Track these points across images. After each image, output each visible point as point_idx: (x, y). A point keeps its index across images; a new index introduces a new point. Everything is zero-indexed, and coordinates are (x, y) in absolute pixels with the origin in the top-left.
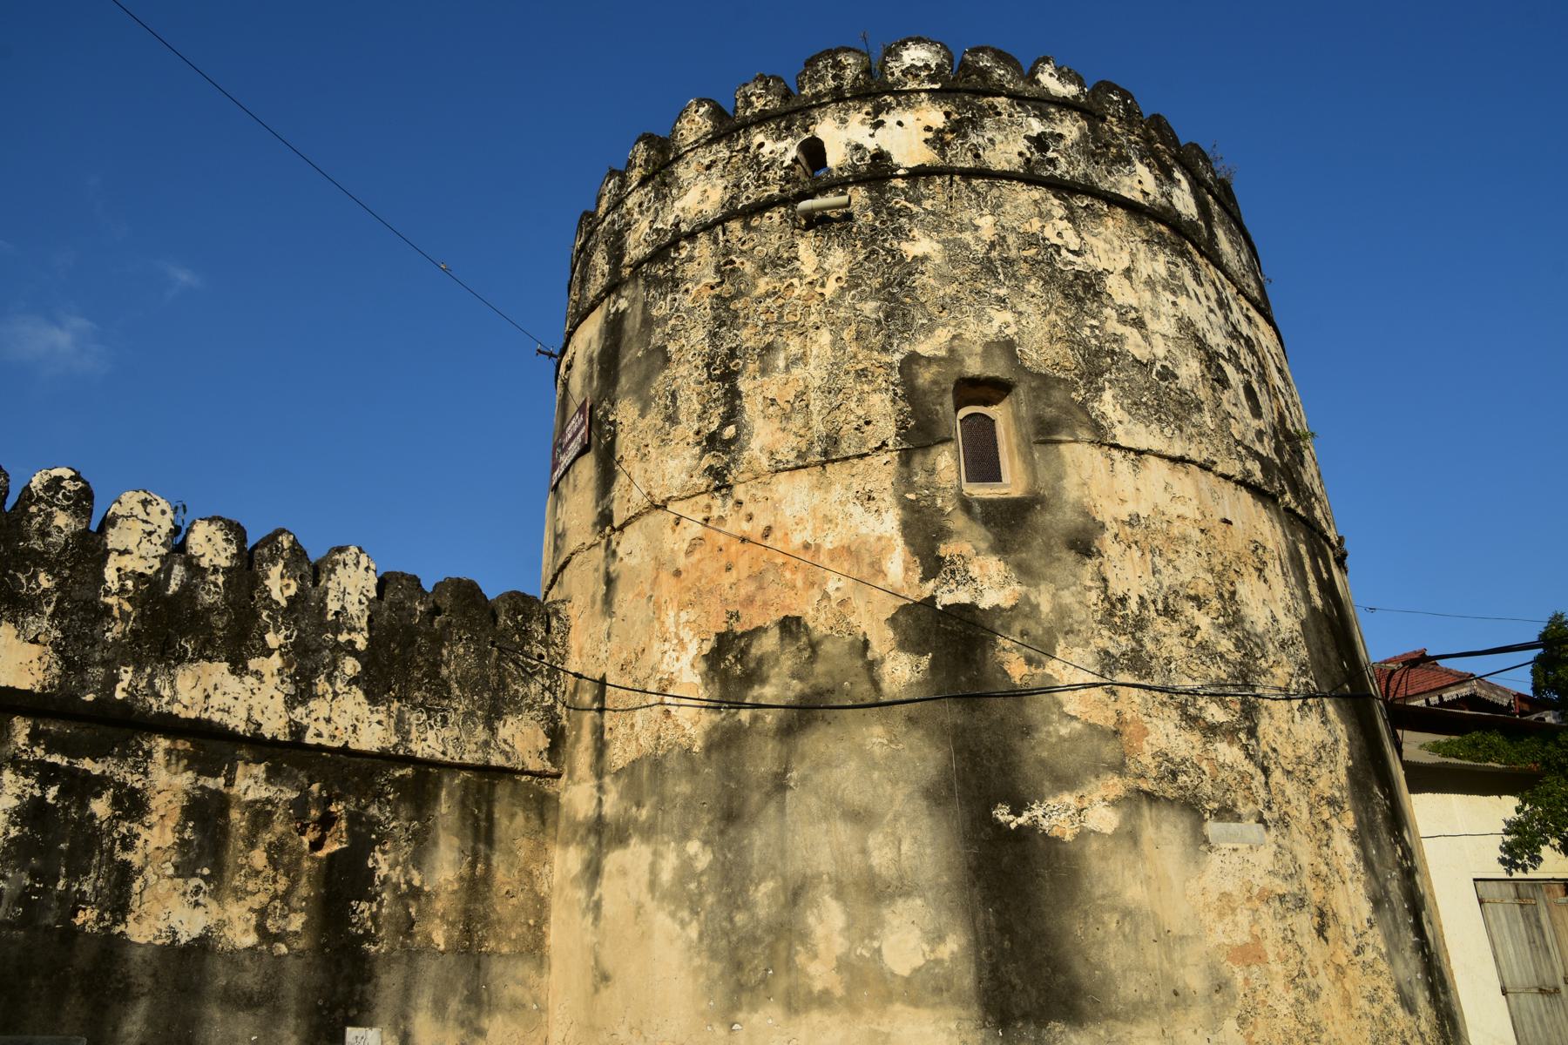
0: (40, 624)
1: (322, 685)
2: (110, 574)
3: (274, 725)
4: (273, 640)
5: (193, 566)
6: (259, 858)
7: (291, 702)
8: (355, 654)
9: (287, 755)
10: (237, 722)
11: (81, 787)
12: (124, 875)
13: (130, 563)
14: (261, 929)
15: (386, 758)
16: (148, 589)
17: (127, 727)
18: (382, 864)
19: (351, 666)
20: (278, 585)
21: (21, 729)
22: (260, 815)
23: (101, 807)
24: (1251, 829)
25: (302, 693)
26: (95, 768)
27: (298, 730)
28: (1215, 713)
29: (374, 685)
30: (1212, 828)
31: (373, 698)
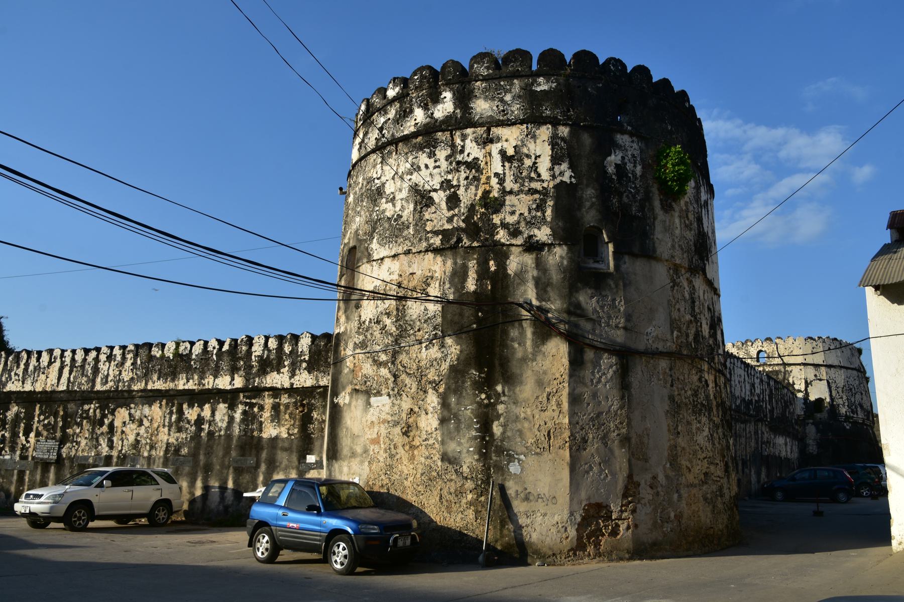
0: (242, 373)
1: (297, 372)
2: (253, 357)
3: (287, 385)
4: (286, 363)
5: (269, 351)
6: (287, 416)
7: (290, 378)
8: (305, 361)
9: (291, 391)
10: (279, 386)
11: (252, 406)
12: (261, 423)
13: (258, 354)
14: (288, 433)
15: (313, 388)
16: (261, 357)
17: (258, 391)
18: (315, 415)
19: (304, 365)
20: (287, 348)
21: (241, 395)
22: (287, 406)
23: (256, 410)
24: (385, 399)
25: (293, 375)
26: (254, 401)
27: (292, 384)
28: (383, 357)
29: (310, 370)
30: (373, 400)
31: (309, 372)
